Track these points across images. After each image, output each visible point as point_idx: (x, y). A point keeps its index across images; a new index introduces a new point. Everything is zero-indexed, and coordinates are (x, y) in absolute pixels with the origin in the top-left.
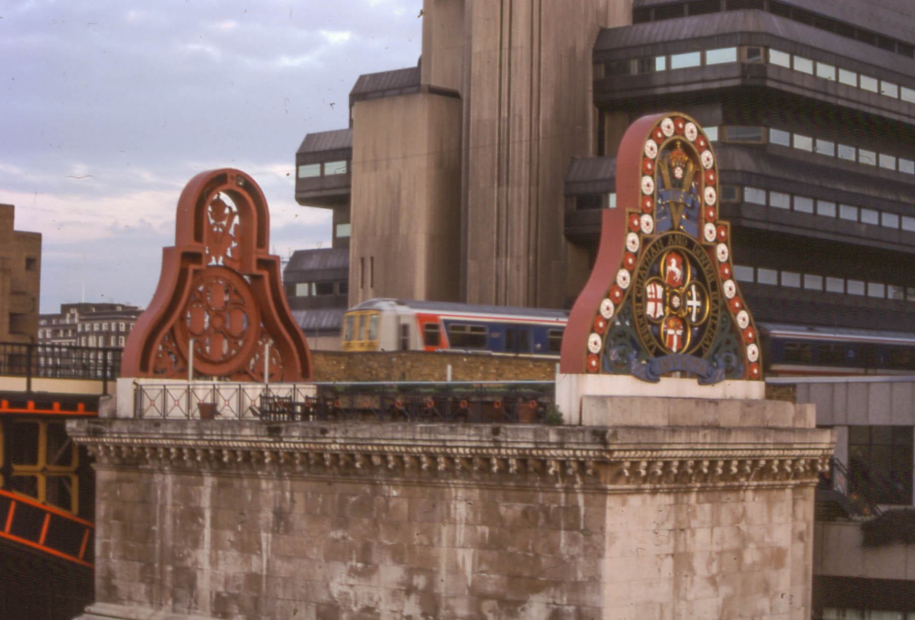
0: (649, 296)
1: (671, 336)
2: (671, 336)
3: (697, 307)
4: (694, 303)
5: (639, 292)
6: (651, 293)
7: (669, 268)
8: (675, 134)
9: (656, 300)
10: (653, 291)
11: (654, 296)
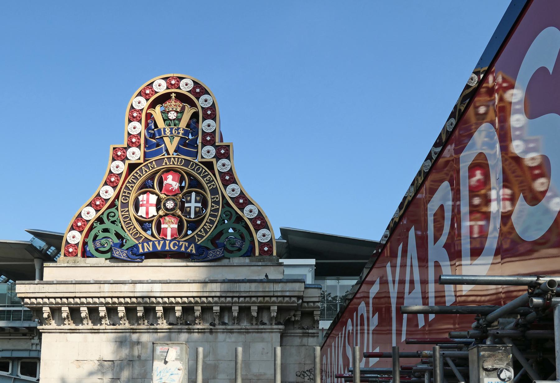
0: (141, 203)
3: (195, 207)
4: (193, 205)
7: (165, 182)
8: (168, 88)
11: (145, 202)
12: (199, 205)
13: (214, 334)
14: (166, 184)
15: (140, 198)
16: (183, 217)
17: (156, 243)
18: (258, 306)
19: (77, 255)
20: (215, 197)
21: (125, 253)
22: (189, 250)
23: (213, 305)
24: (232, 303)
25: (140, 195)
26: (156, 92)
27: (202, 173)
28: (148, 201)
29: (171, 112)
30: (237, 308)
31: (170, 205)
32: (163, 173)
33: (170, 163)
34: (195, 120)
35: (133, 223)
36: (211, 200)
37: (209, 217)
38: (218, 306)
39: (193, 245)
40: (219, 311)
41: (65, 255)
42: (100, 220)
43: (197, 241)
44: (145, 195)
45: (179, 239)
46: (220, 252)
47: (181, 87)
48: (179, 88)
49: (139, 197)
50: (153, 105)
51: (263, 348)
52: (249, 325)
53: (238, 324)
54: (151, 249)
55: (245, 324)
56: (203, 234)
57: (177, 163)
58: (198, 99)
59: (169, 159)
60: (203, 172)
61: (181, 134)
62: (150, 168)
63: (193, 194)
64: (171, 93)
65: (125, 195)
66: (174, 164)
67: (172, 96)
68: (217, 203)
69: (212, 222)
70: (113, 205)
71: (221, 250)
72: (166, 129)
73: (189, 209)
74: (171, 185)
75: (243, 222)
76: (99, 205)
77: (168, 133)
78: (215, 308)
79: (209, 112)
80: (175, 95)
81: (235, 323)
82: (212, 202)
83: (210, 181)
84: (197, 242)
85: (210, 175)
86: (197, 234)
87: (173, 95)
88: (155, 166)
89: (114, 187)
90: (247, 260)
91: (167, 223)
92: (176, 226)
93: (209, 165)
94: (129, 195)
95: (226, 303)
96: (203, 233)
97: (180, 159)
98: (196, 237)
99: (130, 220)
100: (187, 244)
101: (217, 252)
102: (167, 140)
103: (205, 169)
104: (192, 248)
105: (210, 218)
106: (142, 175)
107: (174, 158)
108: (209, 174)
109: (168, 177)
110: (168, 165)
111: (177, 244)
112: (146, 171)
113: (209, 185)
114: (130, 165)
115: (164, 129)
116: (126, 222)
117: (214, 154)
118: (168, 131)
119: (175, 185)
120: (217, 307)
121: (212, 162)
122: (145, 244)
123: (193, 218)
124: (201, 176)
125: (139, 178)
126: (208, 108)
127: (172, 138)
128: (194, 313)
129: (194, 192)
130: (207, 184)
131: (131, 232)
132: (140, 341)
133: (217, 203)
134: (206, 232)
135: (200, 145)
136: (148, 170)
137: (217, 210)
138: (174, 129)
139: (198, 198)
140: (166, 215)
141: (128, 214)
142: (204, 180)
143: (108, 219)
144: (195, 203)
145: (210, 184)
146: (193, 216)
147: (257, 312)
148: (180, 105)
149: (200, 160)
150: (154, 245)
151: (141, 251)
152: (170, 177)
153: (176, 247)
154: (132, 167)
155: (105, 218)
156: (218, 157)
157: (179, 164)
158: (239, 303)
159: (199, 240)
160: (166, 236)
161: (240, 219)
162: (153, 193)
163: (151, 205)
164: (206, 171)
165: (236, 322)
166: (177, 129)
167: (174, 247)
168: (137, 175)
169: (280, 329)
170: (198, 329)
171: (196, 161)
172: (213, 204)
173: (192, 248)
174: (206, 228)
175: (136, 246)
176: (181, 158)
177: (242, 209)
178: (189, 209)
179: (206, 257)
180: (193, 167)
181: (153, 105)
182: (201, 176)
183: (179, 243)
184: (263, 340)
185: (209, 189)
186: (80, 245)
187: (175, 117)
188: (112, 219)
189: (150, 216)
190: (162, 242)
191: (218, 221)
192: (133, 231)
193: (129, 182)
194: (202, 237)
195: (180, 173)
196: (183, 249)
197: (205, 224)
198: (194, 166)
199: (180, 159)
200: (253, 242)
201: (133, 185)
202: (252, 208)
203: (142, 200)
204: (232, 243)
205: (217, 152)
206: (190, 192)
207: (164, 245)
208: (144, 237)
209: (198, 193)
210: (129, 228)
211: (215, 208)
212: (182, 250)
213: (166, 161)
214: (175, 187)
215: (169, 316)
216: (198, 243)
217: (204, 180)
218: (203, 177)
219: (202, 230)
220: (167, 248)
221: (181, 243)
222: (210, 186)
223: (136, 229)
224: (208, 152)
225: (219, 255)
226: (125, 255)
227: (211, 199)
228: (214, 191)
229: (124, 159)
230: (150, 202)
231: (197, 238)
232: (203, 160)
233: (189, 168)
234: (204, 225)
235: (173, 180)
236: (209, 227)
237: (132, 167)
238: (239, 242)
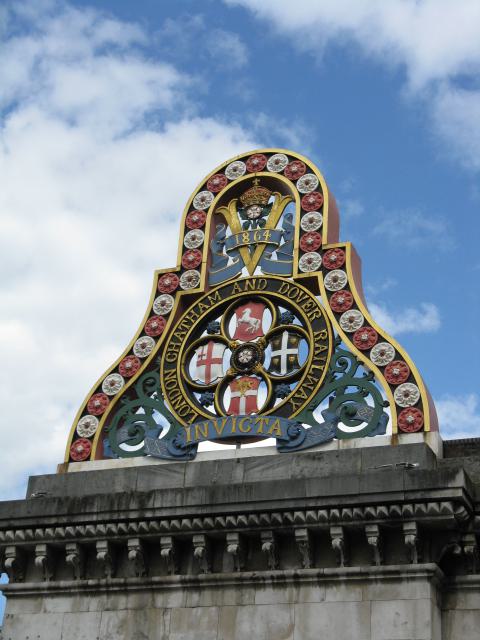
3: (289, 356)
8: (247, 173)
9: (209, 362)
13: (303, 589)
18: (378, 524)
23: (295, 526)
24: (329, 521)
25: (197, 347)
26: (230, 181)
40: (306, 539)
42: (130, 393)
44: (206, 348)
47: (269, 168)
48: (265, 169)
51: (397, 614)
53: (348, 564)
63: (285, 336)
64: (253, 178)
70: (154, 365)
73: (277, 360)
74: (248, 323)
76: (130, 369)
87: (256, 181)
91: (239, 389)
93: (312, 284)
99: (178, 387)
100: (267, 419)
114: (184, 298)
117: (319, 264)
121: (315, 279)
127: (254, 247)
128: (262, 544)
130: (306, 313)
132: (169, 606)
135: (295, 254)
146: (284, 371)
149: (296, 275)
154: (186, 301)
155: (139, 389)
164: (305, 293)
165: (343, 560)
167: (245, 427)
169: (428, 571)
170: (272, 578)
171: (291, 280)
177: (366, 352)
178: (277, 360)
181: (224, 202)
184: (395, 597)
186: (96, 438)
202: (384, 348)
204: (350, 412)
220: (233, 429)
230: (213, 357)
232: (302, 276)
235: (251, 316)
237: (186, 301)
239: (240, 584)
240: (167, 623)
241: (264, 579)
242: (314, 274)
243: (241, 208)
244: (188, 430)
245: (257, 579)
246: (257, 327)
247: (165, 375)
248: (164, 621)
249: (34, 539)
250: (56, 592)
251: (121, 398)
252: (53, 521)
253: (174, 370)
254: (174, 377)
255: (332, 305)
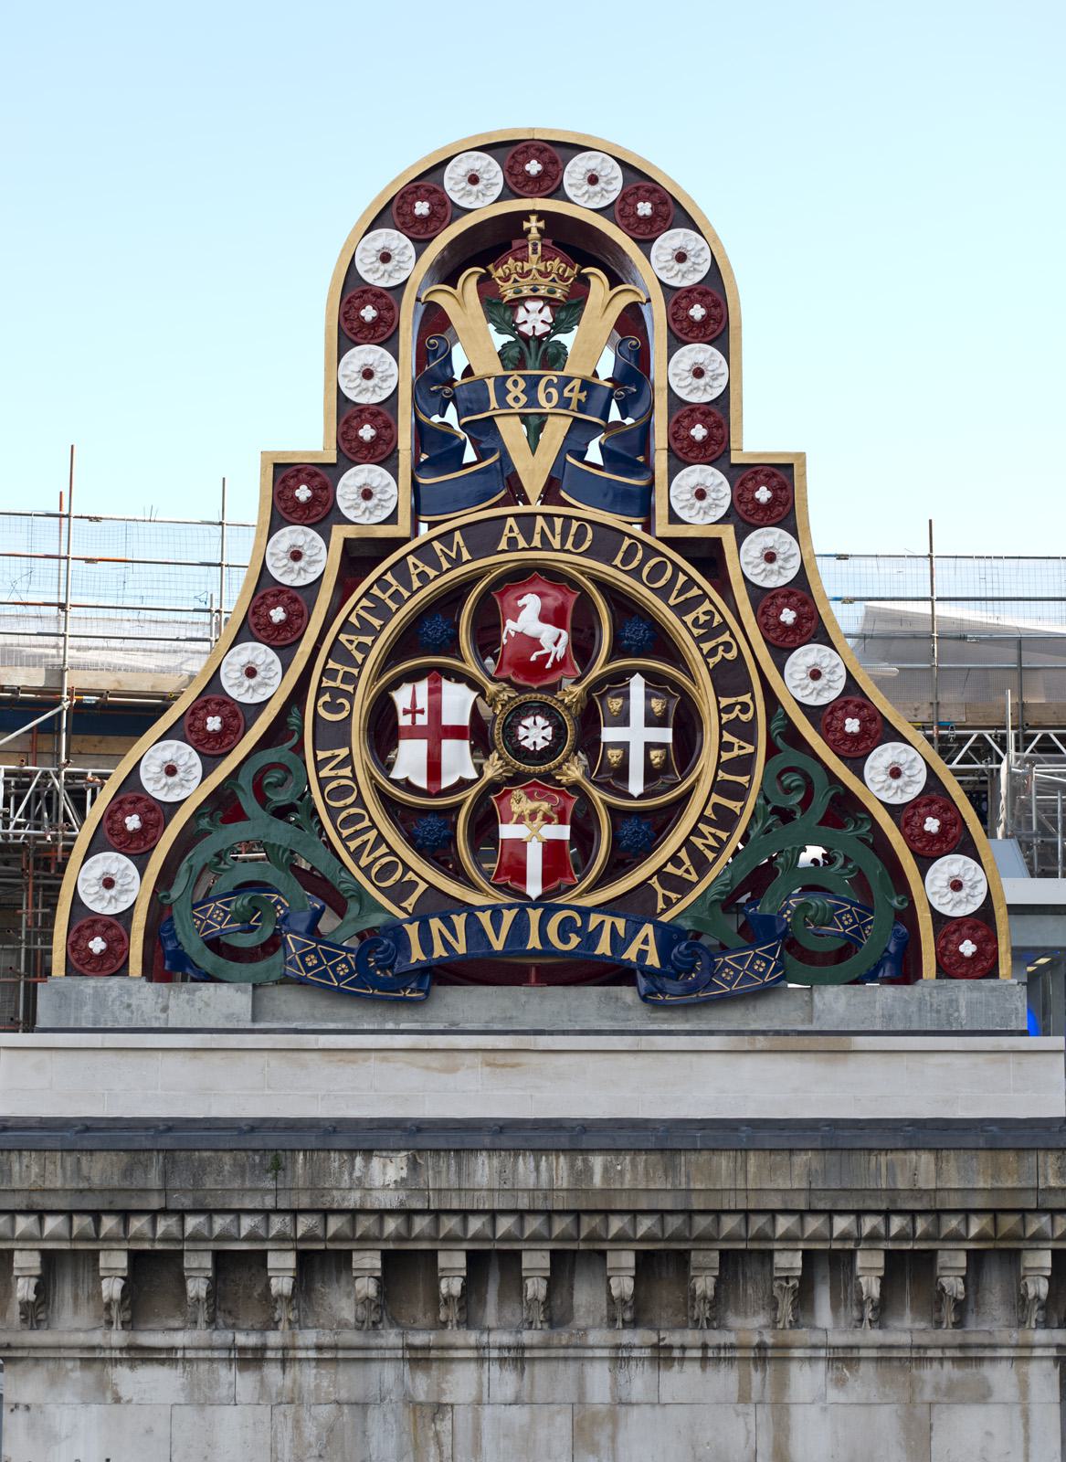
0: (404, 721)
1: (521, 844)
2: (521, 844)
3: (649, 746)
5: (333, 707)
6: (413, 711)
7: (511, 626)
9: (438, 732)
10: (423, 702)
11: (422, 720)
12: (665, 735)
13: (770, 1369)
14: (513, 634)
15: (402, 698)
16: (597, 795)
17: (485, 918)
19: (122, 970)
20: (737, 703)
21: (345, 960)
22: (631, 954)
23: (777, 1246)
24: (858, 1240)
25: (395, 684)
27: (675, 593)
28: (435, 710)
29: (530, 305)
30: (879, 1261)
31: (535, 733)
32: (495, 584)
33: (529, 539)
34: (634, 343)
35: (371, 819)
36: (720, 718)
37: (713, 795)
38: (797, 1250)
39: (648, 929)
40: (799, 1273)
41: (70, 970)
42: (222, 805)
43: (661, 905)
45: (580, 896)
46: (768, 963)
47: (570, 192)
48: (558, 192)
49: (396, 695)
50: (447, 273)
51: (989, 1434)
52: (923, 1325)
54: (461, 948)
55: (906, 1329)
56: (686, 876)
57: (564, 541)
58: (645, 244)
59: (526, 521)
60: (679, 585)
61: (574, 405)
62: (443, 559)
63: (637, 685)
64: (525, 215)
65: (331, 684)
66: (546, 545)
67: (529, 231)
68: (745, 731)
69: (725, 820)
71: (771, 952)
72: (509, 385)
74: (535, 643)
75: (862, 820)
77: (517, 399)
78: (781, 1260)
79: (697, 312)
80: (541, 224)
81: (861, 1320)
82: (722, 727)
83: (711, 631)
84: (664, 911)
85: (712, 602)
86: (659, 872)
87: (533, 225)
88: (466, 556)
89: (285, 650)
90: (883, 998)
91: (520, 820)
92: (563, 832)
93: (707, 556)
94: (350, 688)
95: (831, 1239)
96: (687, 871)
97: (575, 524)
98: (657, 886)
99: (360, 802)
100: (621, 924)
101: (752, 962)
102: (512, 432)
103: (685, 573)
104: (645, 941)
105: (716, 798)
106: (406, 594)
107: (549, 517)
108: (705, 595)
109: (520, 603)
110: (524, 549)
111: (579, 924)
112: (423, 576)
113: (706, 647)
115: (501, 381)
116: (344, 815)
117: (726, 502)
118: (516, 391)
119: (554, 642)
120: (790, 1254)
121: (719, 540)
122: (435, 924)
123: (641, 797)
124: (672, 602)
125: (394, 607)
126: (690, 290)
129: (638, 676)
131: (364, 861)
132: (446, 1399)
133: (745, 731)
134: (702, 865)
135: (661, 461)
136: (432, 573)
137: (745, 765)
138: (543, 382)
139: (657, 705)
140: (516, 779)
141: (351, 775)
142: (684, 623)
143: (262, 799)
144: (646, 726)
145: (712, 644)
146: (636, 785)
147: (962, 1277)
148: (564, 271)
149: (663, 528)
150: (474, 929)
151: (417, 954)
152: (531, 604)
153: (575, 941)
156: (746, 517)
157: (569, 546)
158: (887, 1238)
159: (669, 903)
160: (522, 879)
161: (846, 807)
162: (460, 677)
163: (456, 732)
164: (691, 582)
165: (869, 1315)
166: (555, 380)
168: (384, 593)
172: (727, 737)
173: (645, 941)
174: (702, 848)
175: (396, 932)
176: (578, 519)
177: (857, 765)
179: (709, 985)
180: (635, 563)
181: (447, 273)
182: (668, 605)
183: (586, 922)
184: (983, 1396)
185: (707, 664)
187: (548, 328)
188: (281, 797)
189: (447, 782)
190: (509, 917)
191: (753, 814)
192: (377, 854)
193: (346, 627)
194: (683, 887)
195: (575, 584)
196: (604, 947)
197: (695, 826)
198: (640, 555)
199: (575, 524)
200: (907, 916)
201: (368, 640)
203: (408, 707)
205: (737, 499)
206: (617, 681)
207: (520, 927)
208: (422, 886)
209: (653, 678)
210: (357, 842)
211: (736, 752)
212: (598, 952)
213: (511, 530)
214: (554, 649)
215: (572, 1287)
216: (665, 918)
217: (684, 623)
218: (679, 610)
219: (683, 854)
220: (534, 942)
221: (595, 920)
222: (713, 652)
223: (388, 846)
224: (701, 495)
225: (761, 975)
226: (342, 969)
227: (720, 711)
228: (730, 677)
229: (322, 514)
231: (660, 891)
233: (616, 567)
234: (691, 833)
235: (544, 618)
236: (712, 842)
238: (849, 912)
239: (620, 1358)
240: (446, 1440)
241: (683, 1348)
242: (714, 532)
243: (499, 309)
244: (412, 930)
245: (670, 1347)
246: (560, 651)
247: (319, 765)
248: (437, 1434)
249: (96, 1239)
250: (139, 1356)
251: (197, 814)
252: (155, 1203)
253: (343, 752)
254: (347, 772)
255: (764, 628)
